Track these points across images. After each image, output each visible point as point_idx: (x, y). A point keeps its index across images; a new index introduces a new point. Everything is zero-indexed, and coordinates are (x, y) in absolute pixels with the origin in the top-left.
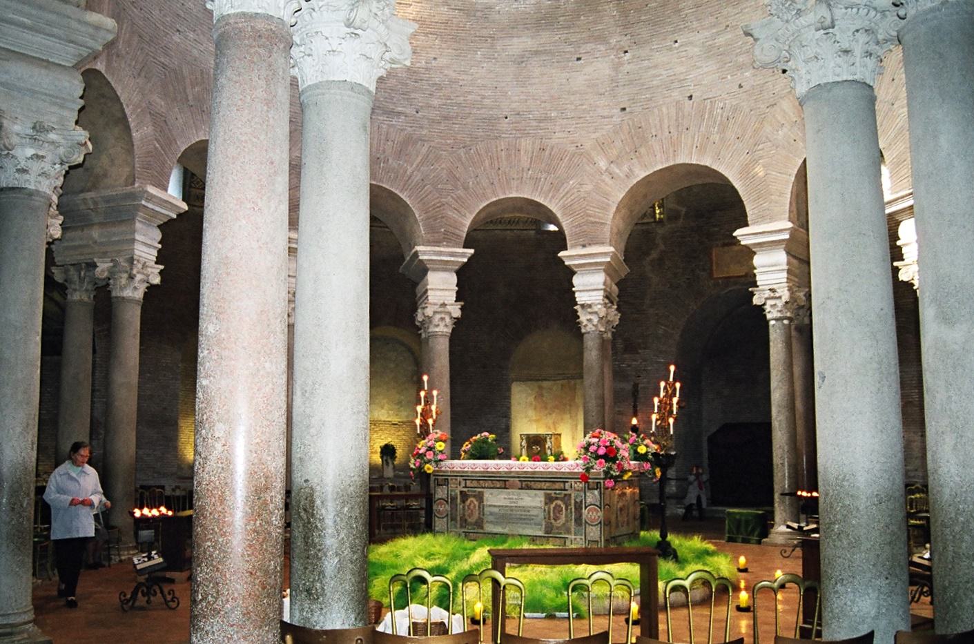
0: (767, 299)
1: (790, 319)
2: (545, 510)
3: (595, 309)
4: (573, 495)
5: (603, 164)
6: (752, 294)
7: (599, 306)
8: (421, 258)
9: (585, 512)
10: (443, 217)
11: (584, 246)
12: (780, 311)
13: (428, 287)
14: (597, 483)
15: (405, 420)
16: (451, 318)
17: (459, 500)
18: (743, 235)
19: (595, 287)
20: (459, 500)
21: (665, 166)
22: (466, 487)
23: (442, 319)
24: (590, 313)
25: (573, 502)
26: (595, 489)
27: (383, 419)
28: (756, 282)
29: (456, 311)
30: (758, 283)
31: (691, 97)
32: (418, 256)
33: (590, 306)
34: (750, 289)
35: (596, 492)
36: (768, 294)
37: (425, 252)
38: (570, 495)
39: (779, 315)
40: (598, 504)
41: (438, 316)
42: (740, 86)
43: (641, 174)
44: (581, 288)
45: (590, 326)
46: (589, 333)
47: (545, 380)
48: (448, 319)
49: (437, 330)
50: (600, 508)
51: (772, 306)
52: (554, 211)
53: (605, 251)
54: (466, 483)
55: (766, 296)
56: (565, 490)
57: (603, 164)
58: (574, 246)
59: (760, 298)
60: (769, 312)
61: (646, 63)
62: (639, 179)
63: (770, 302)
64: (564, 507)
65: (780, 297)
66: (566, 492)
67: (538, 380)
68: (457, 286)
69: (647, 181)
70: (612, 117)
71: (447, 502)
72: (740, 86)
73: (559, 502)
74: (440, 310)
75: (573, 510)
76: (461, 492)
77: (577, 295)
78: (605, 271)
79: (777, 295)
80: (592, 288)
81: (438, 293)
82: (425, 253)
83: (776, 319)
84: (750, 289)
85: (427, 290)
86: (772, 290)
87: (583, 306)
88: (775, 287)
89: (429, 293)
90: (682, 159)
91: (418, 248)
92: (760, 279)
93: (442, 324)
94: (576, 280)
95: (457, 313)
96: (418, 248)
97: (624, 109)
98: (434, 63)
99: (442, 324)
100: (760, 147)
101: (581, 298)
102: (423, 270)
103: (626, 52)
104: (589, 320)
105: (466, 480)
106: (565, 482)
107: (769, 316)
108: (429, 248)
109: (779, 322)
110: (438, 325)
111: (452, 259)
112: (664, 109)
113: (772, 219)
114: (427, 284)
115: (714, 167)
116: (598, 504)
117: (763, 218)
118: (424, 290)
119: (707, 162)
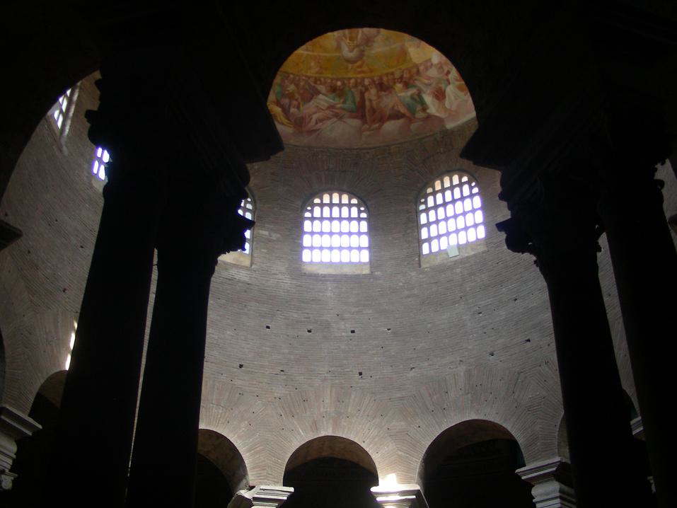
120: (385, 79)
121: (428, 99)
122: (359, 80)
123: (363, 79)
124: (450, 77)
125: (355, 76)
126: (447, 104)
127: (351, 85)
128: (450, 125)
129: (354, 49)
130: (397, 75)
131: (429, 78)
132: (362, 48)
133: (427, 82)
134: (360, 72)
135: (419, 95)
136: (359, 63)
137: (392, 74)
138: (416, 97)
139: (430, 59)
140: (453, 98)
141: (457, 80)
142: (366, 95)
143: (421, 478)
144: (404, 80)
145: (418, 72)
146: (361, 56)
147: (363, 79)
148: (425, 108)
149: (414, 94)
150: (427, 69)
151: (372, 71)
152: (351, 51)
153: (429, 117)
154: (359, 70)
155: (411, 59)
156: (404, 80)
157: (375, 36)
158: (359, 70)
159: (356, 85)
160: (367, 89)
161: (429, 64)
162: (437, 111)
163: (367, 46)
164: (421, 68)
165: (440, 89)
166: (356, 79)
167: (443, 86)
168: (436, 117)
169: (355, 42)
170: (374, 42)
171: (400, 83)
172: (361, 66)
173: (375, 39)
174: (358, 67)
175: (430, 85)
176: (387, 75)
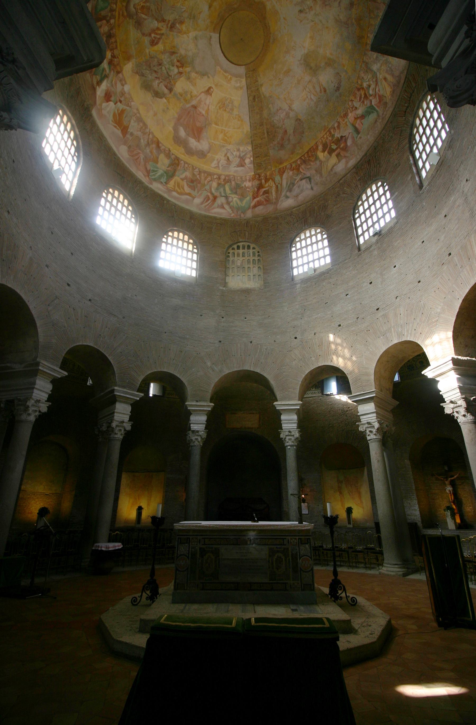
0: (286, 436)
1: (295, 446)
2: (269, 561)
3: (200, 433)
4: (290, 549)
5: (209, 364)
6: (279, 434)
7: (203, 432)
8: (115, 393)
9: (300, 561)
10: (129, 374)
11: (197, 401)
12: (293, 442)
13: (115, 411)
14: (308, 539)
15: (54, 492)
16: (125, 430)
17: (198, 556)
18: (279, 405)
19: (201, 422)
20: (198, 556)
21: (238, 369)
22: (205, 544)
23: (120, 430)
24: (197, 435)
25: (290, 554)
26: (306, 544)
27: (40, 491)
28: (282, 427)
29: (128, 427)
30: (283, 428)
31: (251, 342)
32: (114, 392)
33: (198, 432)
34: (357, 423)
35: (307, 546)
36: (287, 433)
37: (119, 391)
38: (288, 549)
39: (293, 444)
40: (309, 555)
41: (118, 428)
42: (275, 341)
43: (227, 371)
44: (194, 422)
45: (196, 442)
46: (195, 446)
47: (137, 472)
48: (123, 431)
49: (116, 436)
50: (311, 558)
51: (289, 439)
52: (184, 382)
53: (208, 406)
54: (205, 541)
55: (287, 434)
56: (284, 545)
57: (209, 364)
58: (193, 401)
59: (284, 435)
60: (369, 435)
61: (232, 324)
62: (225, 373)
63: (288, 438)
64: (283, 558)
65: (293, 436)
66: (283, 546)
67: (133, 472)
68: (130, 412)
69: (227, 376)
70: (215, 344)
71: (188, 557)
72: (275, 341)
73: (280, 555)
74: (120, 424)
75: (291, 560)
76: (200, 548)
77: (191, 425)
78: (207, 415)
79: (292, 434)
80: (199, 422)
81: (121, 415)
82: (118, 391)
83: (290, 446)
84: (357, 423)
85: (114, 413)
86: (290, 432)
87: (193, 432)
88: (291, 430)
89: (115, 414)
90: (247, 368)
91: (116, 388)
92: (284, 426)
93: (119, 433)
94: (192, 418)
95: (128, 428)
96: (116, 388)
97: (220, 342)
98: (135, 297)
99: (119, 433)
100: (284, 367)
101: (194, 427)
102: (113, 400)
103: (223, 318)
104: (196, 439)
105: (205, 538)
106: (283, 539)
107: (287, 444)
108: (121, 389)
109: (292, 447)
110: (116, 434)
111: (132, 397)
112: (239, 345)
113: (290, 399)
114: (115, 409)
115: (262, 373)
116: (309, 555)
117: (283, 399)
118: (111, 412)
119: (258, 370)
120: (113, 40)
121: (104, 85)
122: (114, 13)
123: (114, 18)
124: (119, 103)
125: (117, 10)
126: (104, 105)
127: (112, 5)
128: (94, 113)
129: (135, 8)
130: (116, 52)
131: (116, 84)
132: (135, 17)
133: (114, 82)
134: (119, 14)
135: (106, 76)
136: (125, 14)
137: (116, 48)
138: (104, 73)
139: (126, 83)
140: (108, 109)
141: (118, 110)
142: (104, 22)
143: (114, 240)
144: (113, 59)
145: (118, 72)
146: (130, 16)
147: (114, 18)
148: (99, 83)
149: (106, 71)
150: (121, 81)
151: (119, 26)
152: (134, 5)
153: (94, 89)
154: (121, 13)
155: (125, 64)
156: (113, 59)
157: (141, 31)
158: (121, 13)
159: (112, 10)
160: (108, 22)
161: (124, 82)
162: (99, 96)
163: (135, 22)
164: (120, 75)
165: (111, 96)
166: (115, 10)
167: (112, 99)
168: (96, 97)
169: (140, 11)
170: (137, 29)
171: (112, 56)
172: (123, 15)
173: (139, 31)
174: (123, 12)
175: (112, 86)
176: (116, 42)
